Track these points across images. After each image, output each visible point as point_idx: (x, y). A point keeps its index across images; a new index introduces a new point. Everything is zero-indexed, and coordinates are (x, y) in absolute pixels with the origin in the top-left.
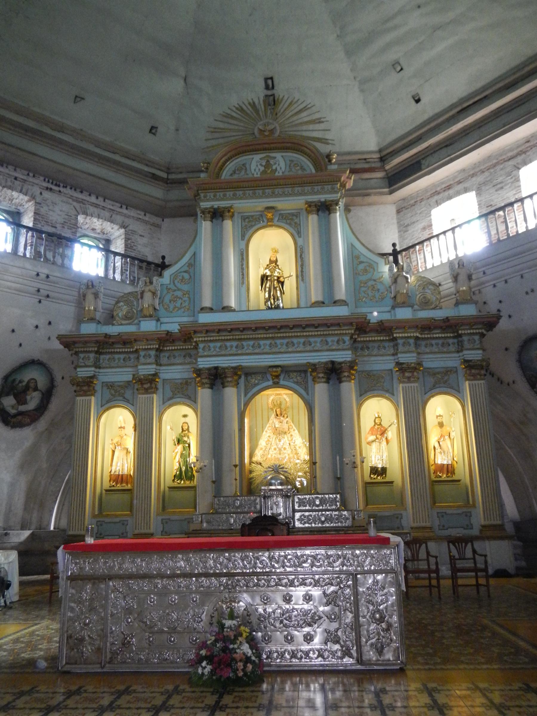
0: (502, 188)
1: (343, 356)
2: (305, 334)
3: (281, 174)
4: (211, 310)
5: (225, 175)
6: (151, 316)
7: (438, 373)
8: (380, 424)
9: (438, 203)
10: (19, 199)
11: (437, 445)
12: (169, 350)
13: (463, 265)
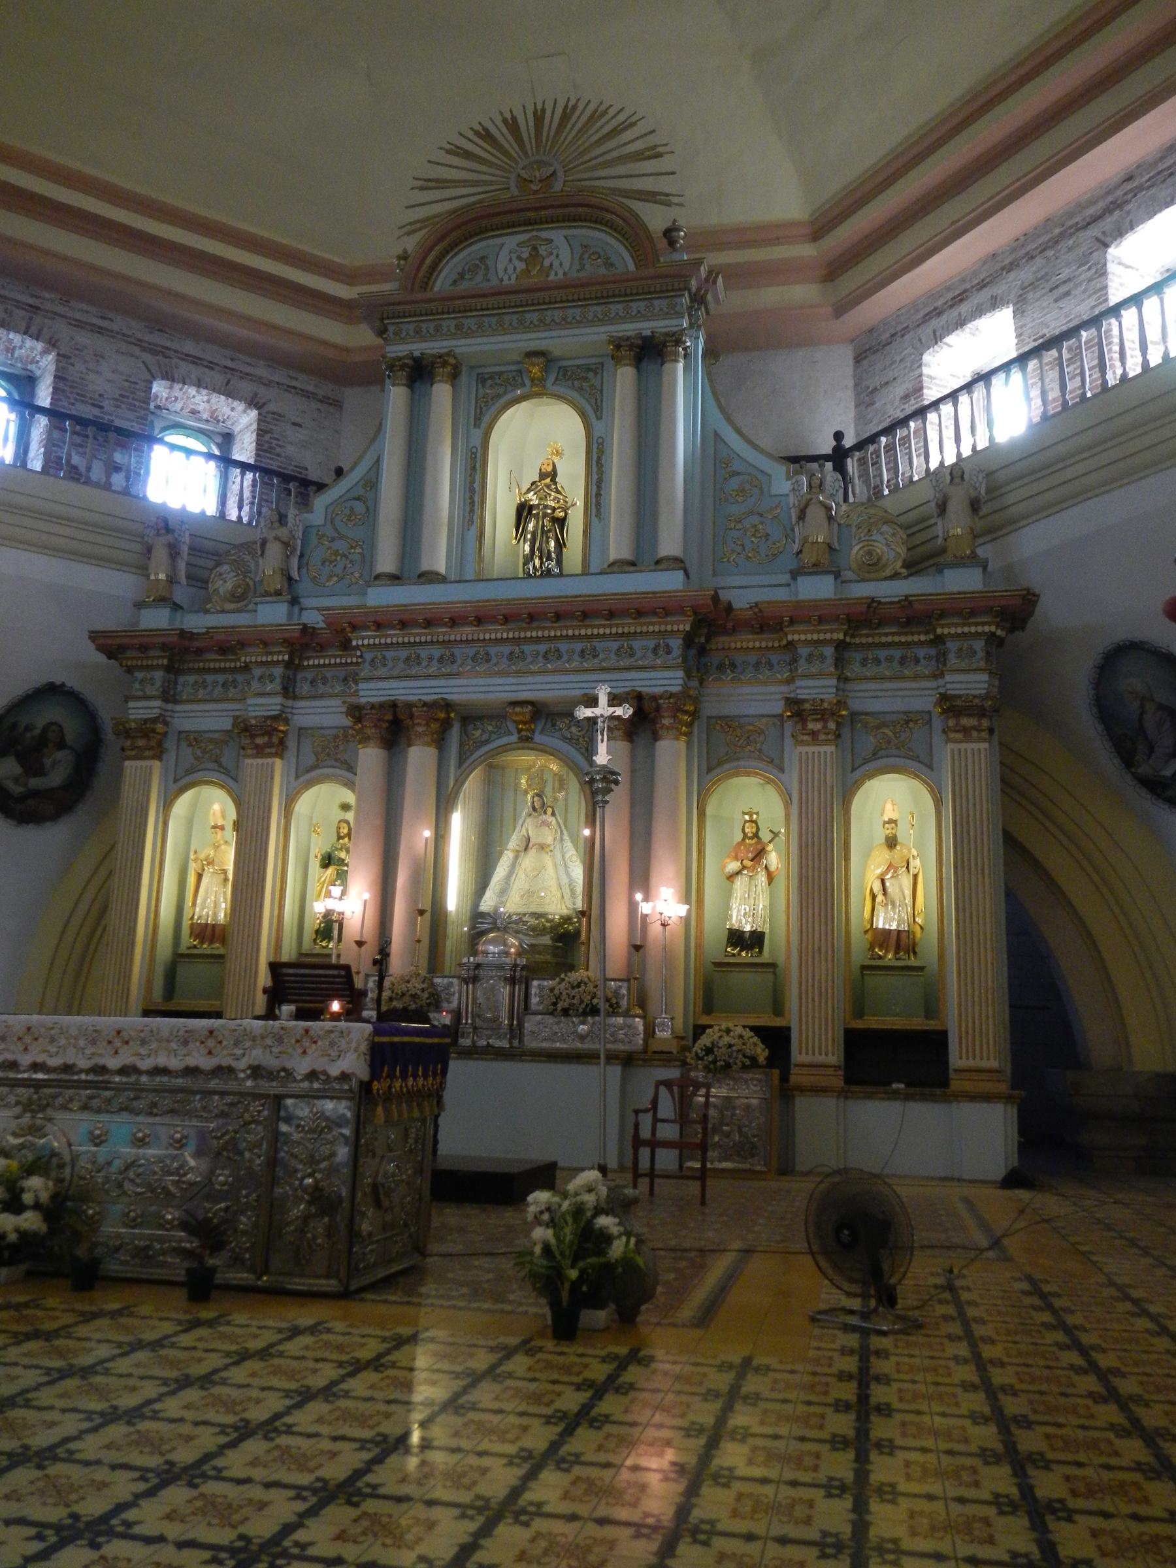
0: (1068, 294)
2: (583, 632)
3: (561, 275)
4: (395, 578)
5: (442, 283)
6: (278, 593)
7: (884, 725)
8: (756, 835)
9: (937, 338)
10: (29, 347)
11: (877, 887)
12: (319, 666)
13: (962, 478)
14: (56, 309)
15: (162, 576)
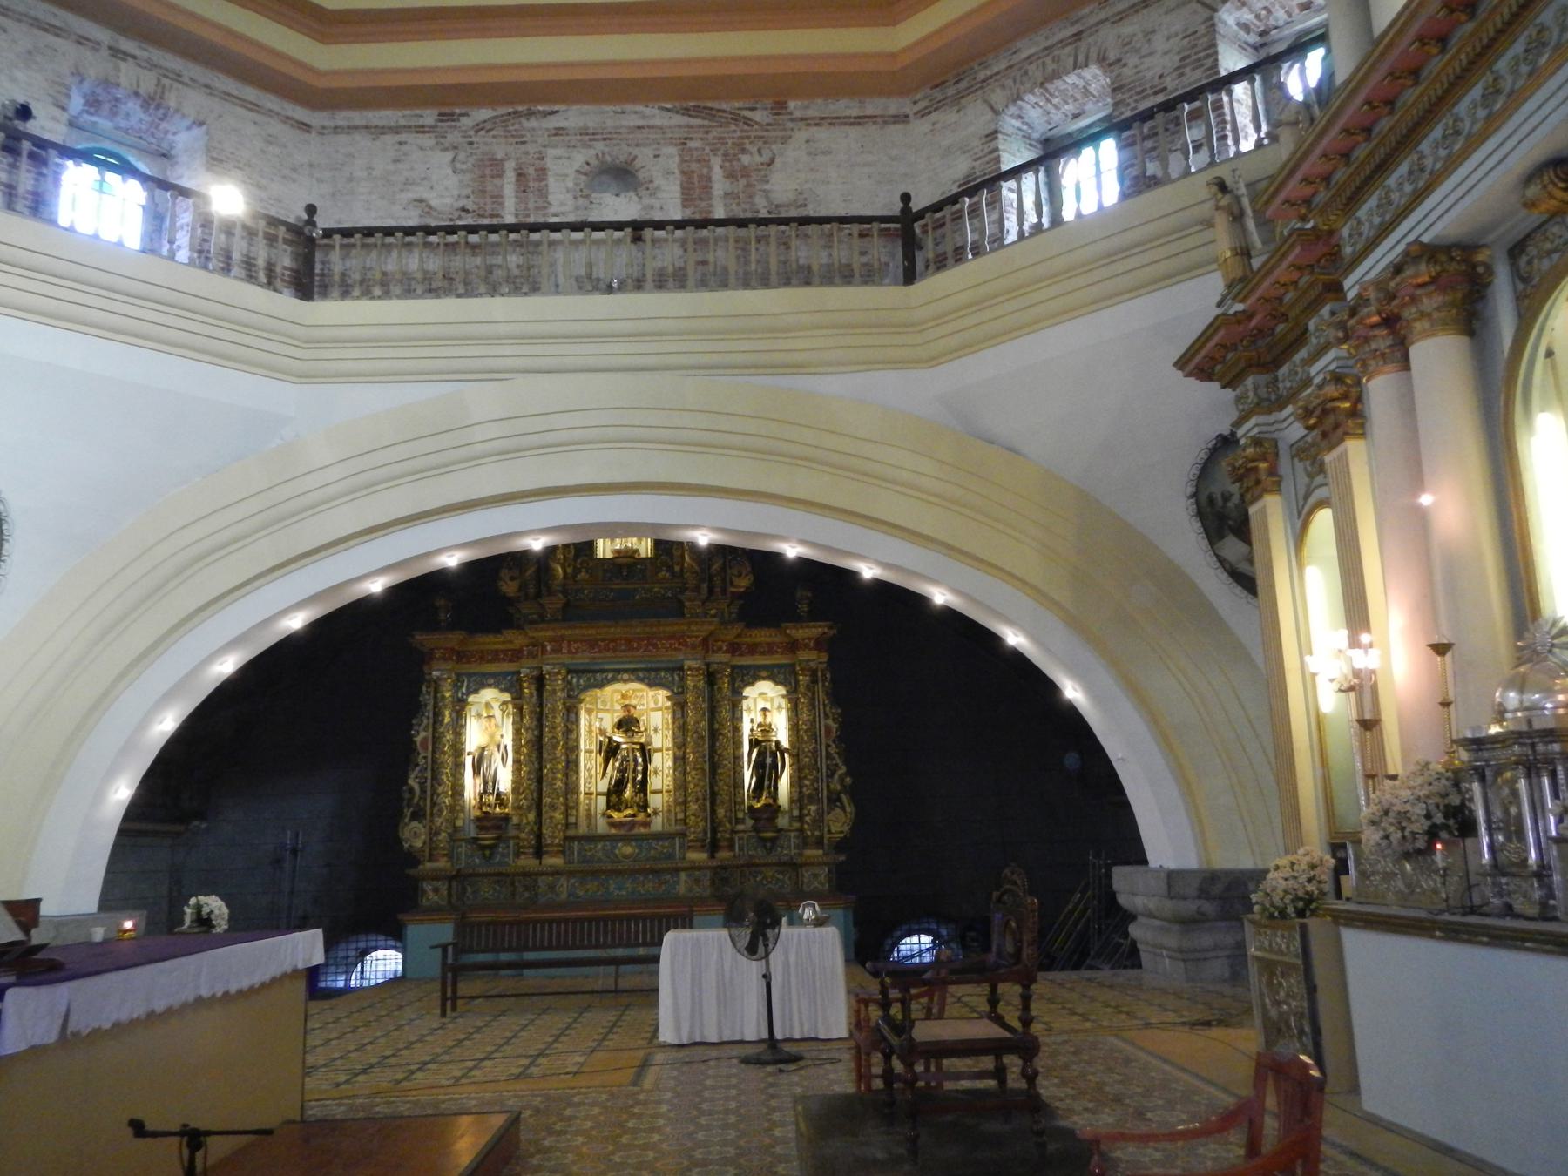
14: (1102, 15)
15: (1228, 254)
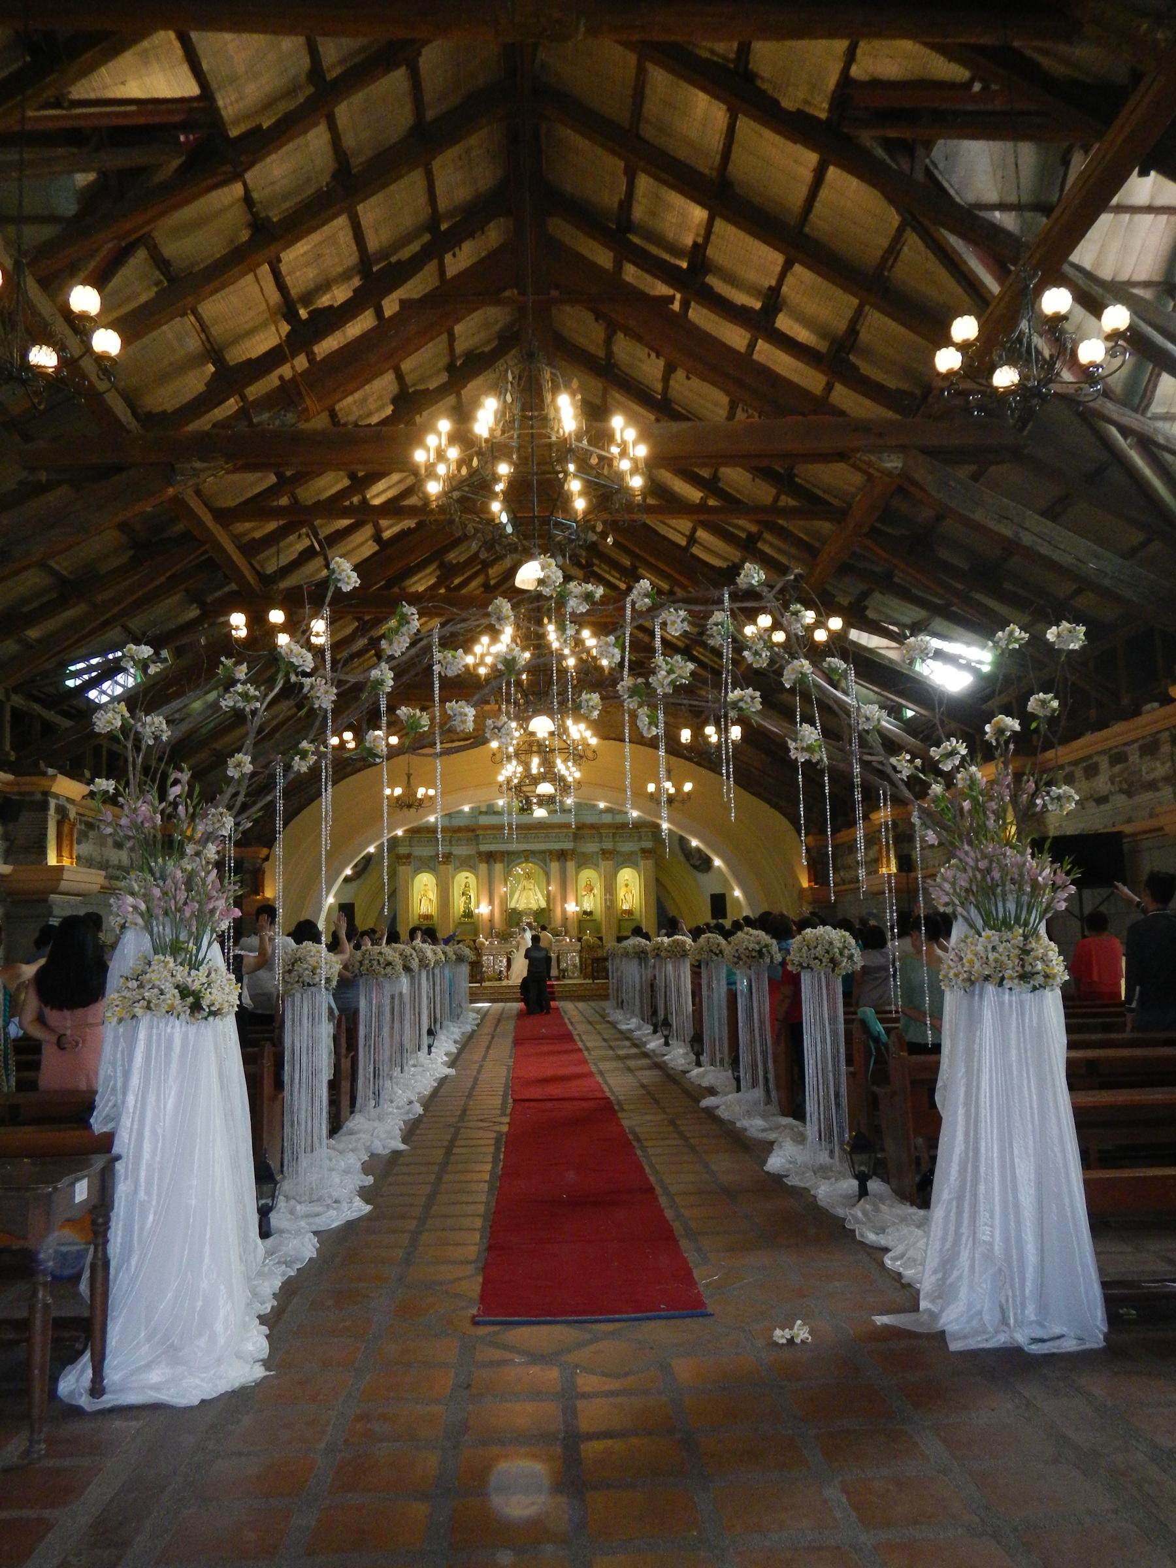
1: (568, 845)
4: (486, 813)
